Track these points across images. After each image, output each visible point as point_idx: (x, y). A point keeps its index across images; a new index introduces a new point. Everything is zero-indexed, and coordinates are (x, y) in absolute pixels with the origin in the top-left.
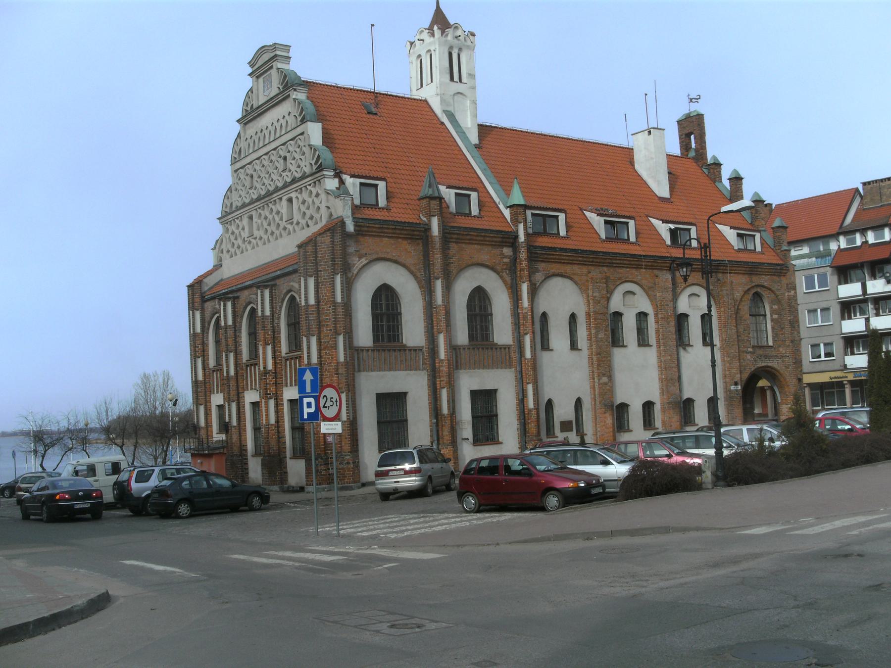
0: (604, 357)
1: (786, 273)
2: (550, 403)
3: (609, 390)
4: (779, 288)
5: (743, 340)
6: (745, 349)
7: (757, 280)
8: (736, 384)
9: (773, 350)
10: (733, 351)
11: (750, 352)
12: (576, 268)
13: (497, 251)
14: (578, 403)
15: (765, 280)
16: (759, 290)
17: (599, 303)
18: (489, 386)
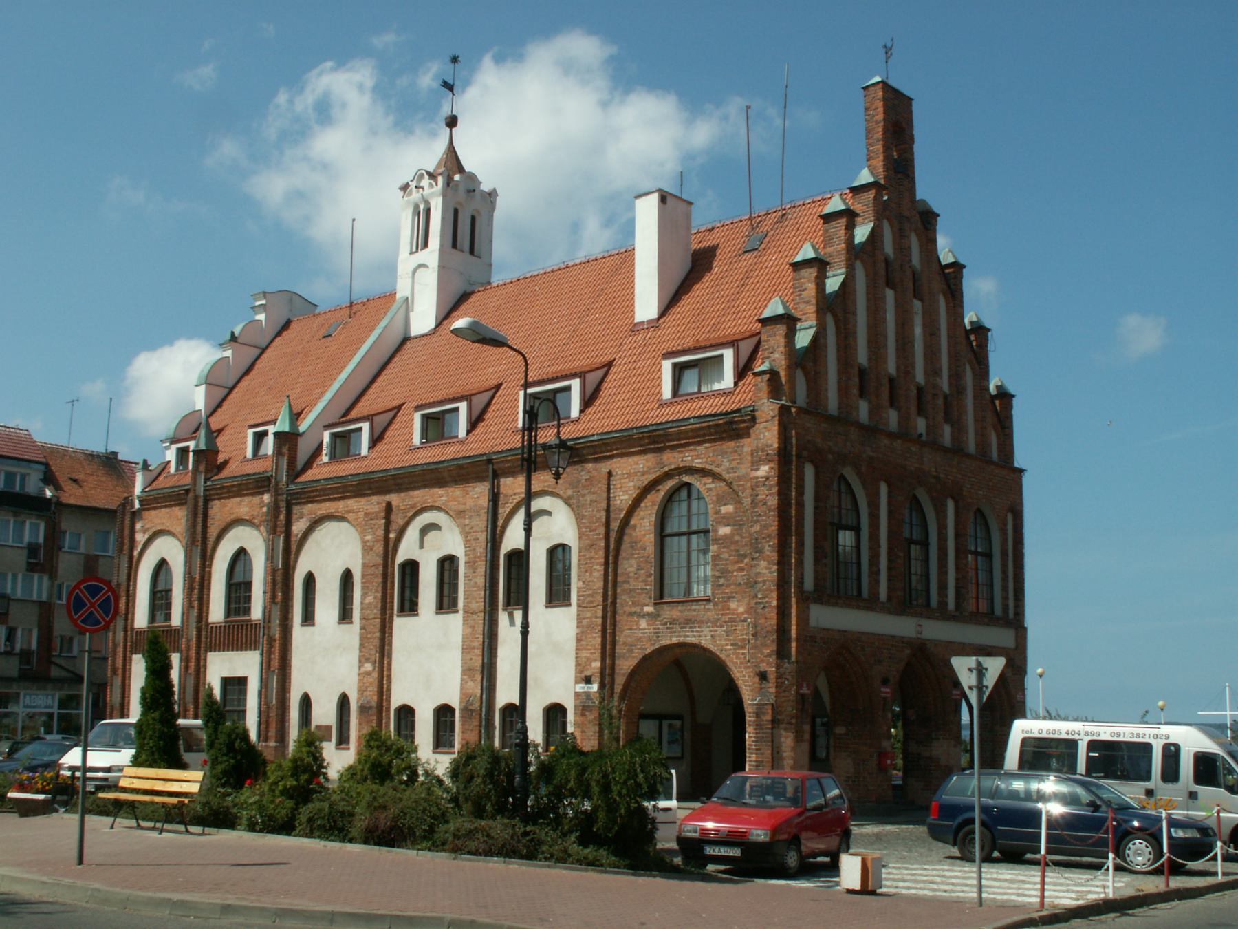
0: (370, 632)
1: (749, 428)
2: (306, 702)
3: (371, 683)
4: (734, 464)
5: (631, 590)
6: (637, 609)
7: (672, 459)
8: (588, 680)
9: (710, 606)
10: (589, 615)
11: (648, 614)
12: (352, 503)
13: (256, 499)
14: (344, 701)
15: (696, 456)
16: (686, 479)
17: (371, 550)
18: (239, 673)
